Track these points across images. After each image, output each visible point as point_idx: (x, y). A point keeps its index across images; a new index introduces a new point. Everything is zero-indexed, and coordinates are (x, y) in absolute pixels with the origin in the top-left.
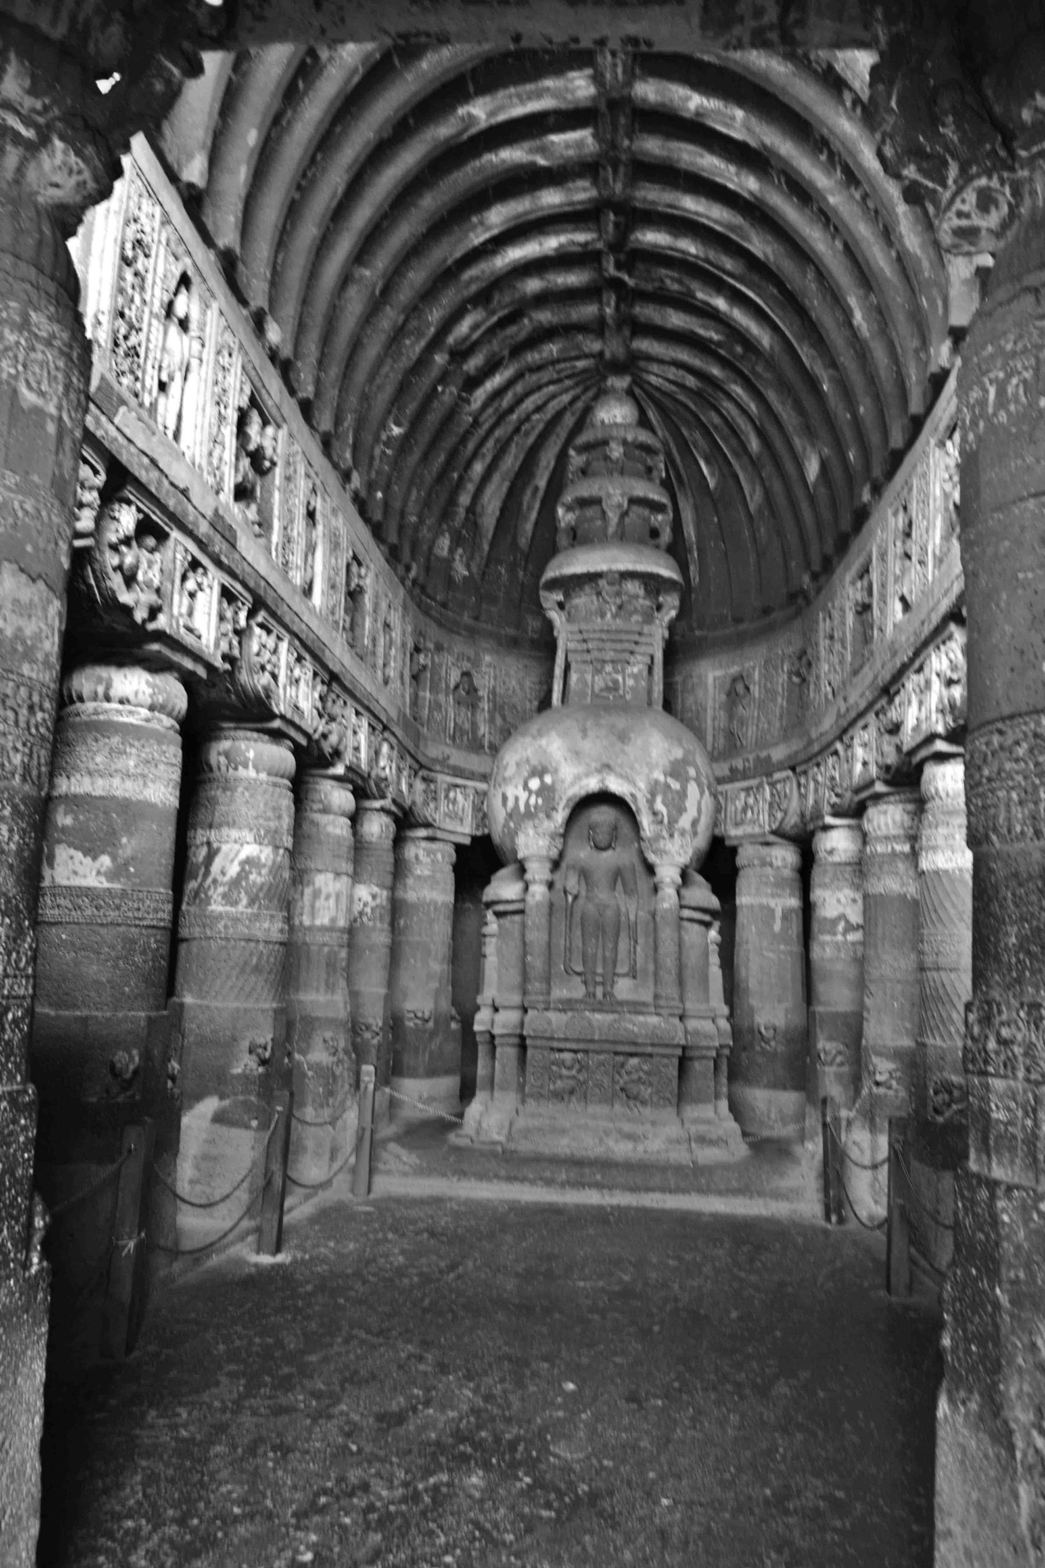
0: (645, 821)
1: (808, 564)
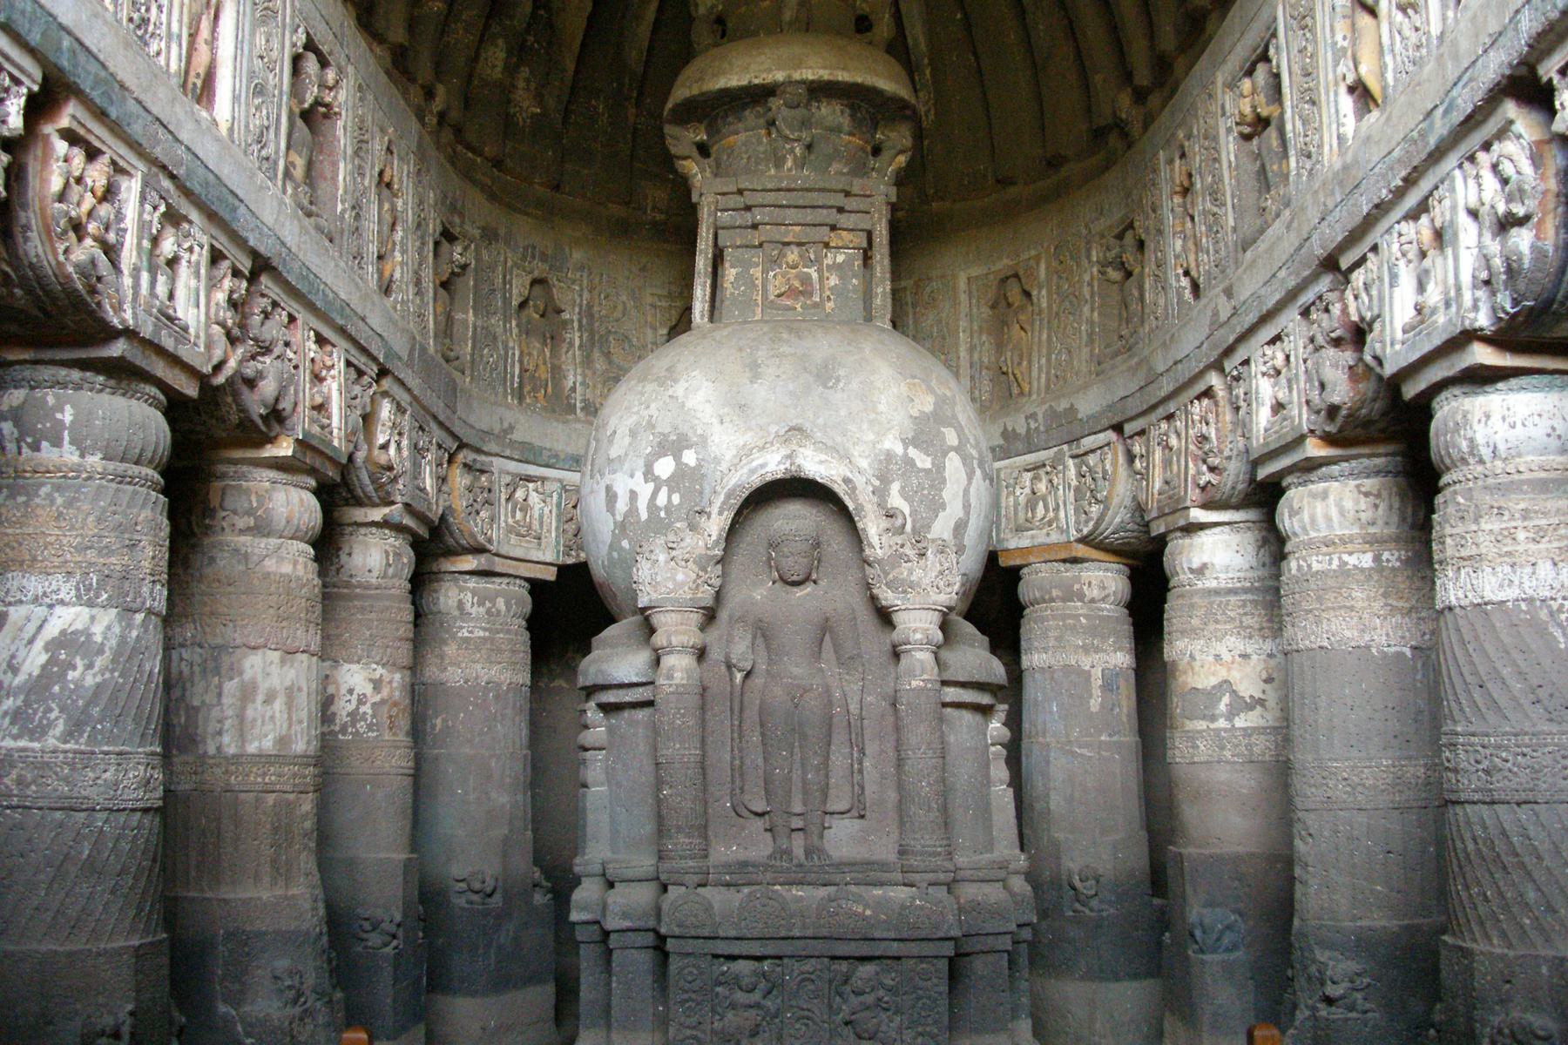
0: (872, 527)
1: (1128, 76)
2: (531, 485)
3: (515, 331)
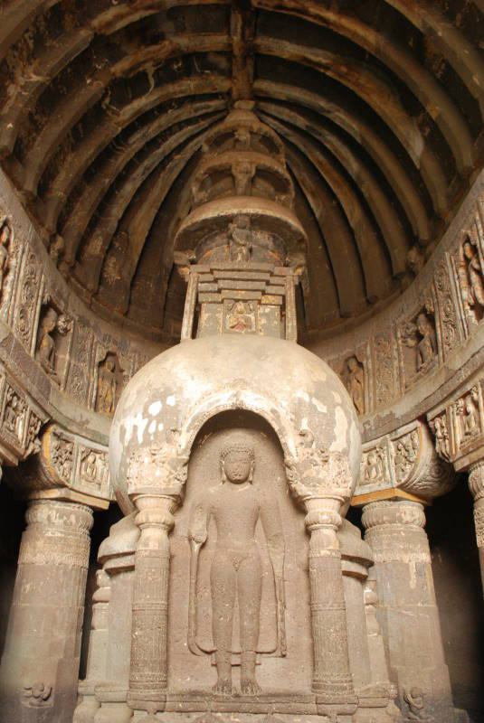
0: (290, 442)
1: (412, 240)
2: (98, 456)
3: (96, 374)
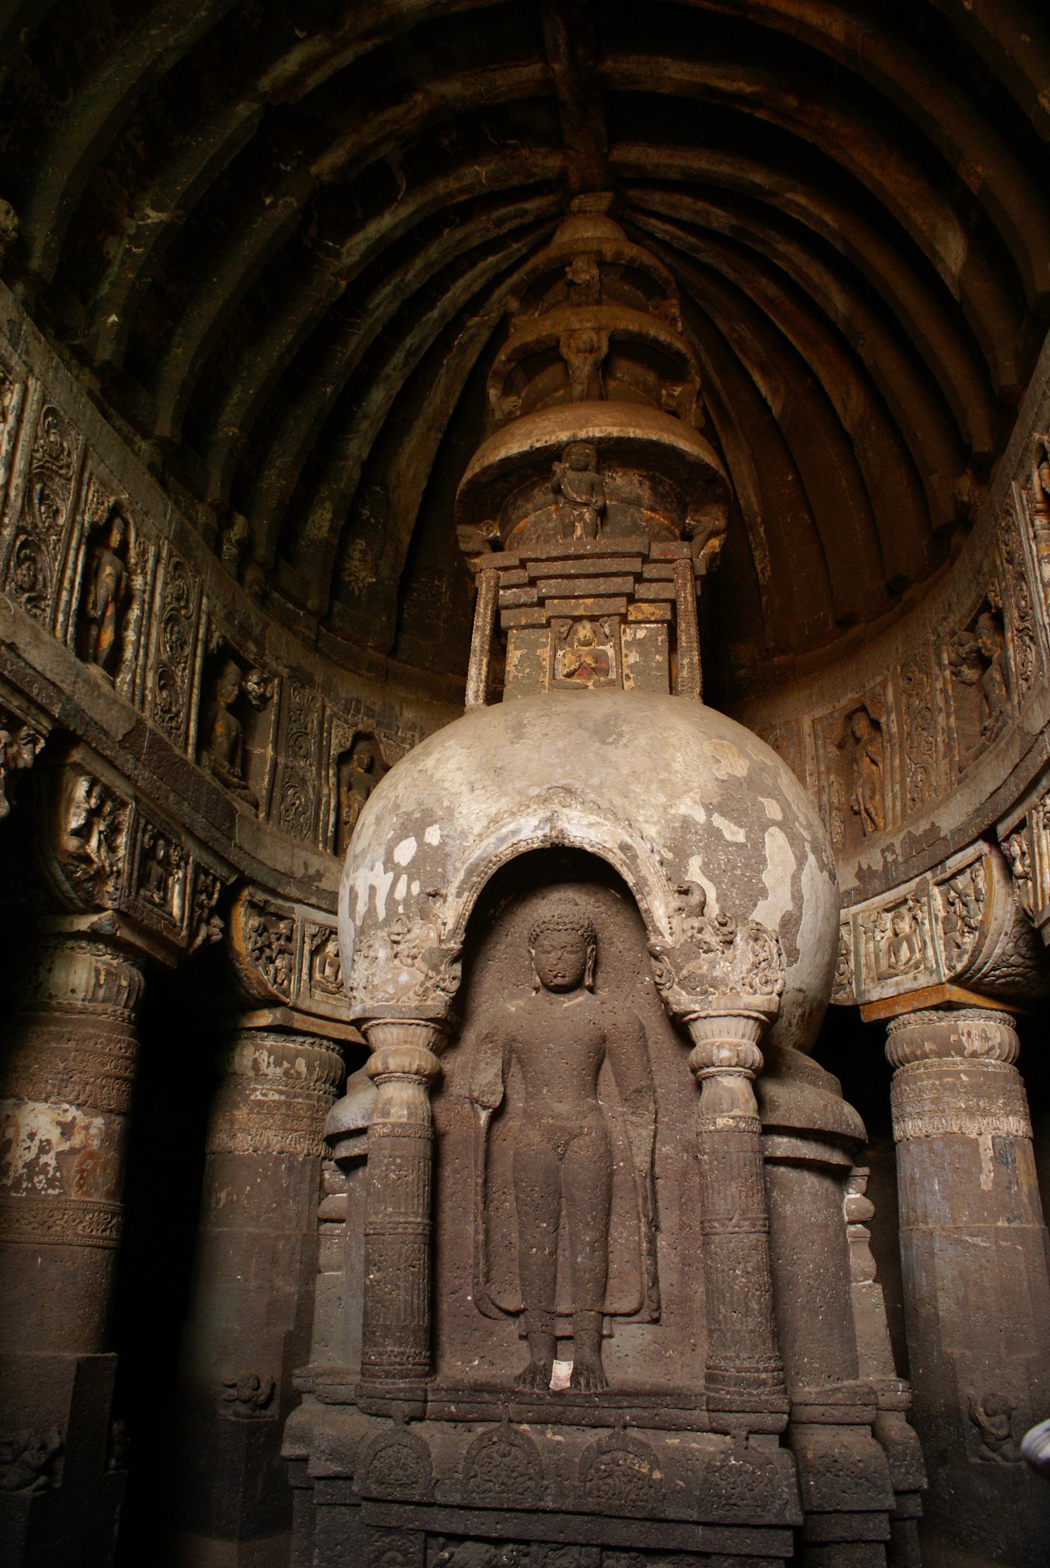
0: (659, 906)
3: (332, 780)
